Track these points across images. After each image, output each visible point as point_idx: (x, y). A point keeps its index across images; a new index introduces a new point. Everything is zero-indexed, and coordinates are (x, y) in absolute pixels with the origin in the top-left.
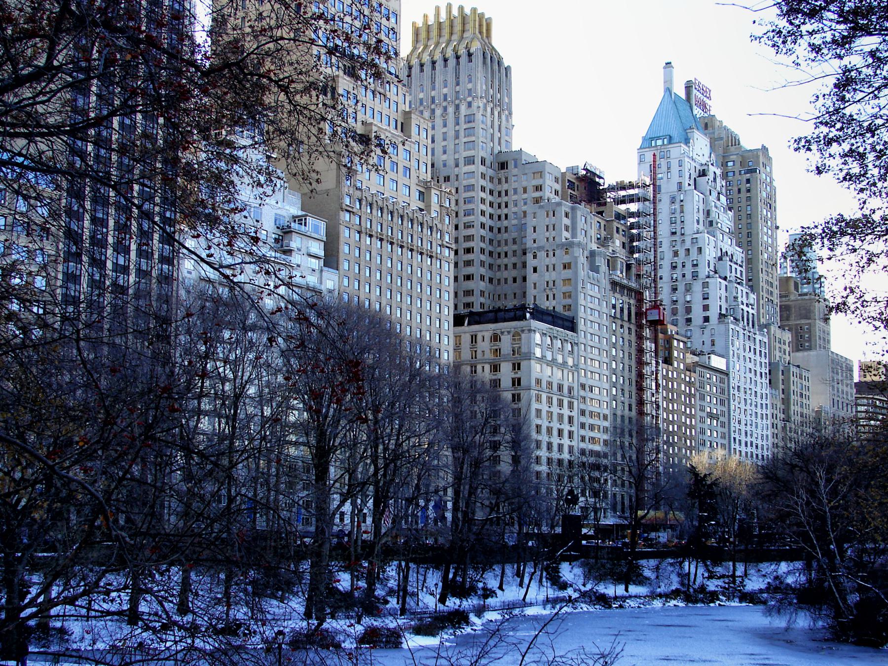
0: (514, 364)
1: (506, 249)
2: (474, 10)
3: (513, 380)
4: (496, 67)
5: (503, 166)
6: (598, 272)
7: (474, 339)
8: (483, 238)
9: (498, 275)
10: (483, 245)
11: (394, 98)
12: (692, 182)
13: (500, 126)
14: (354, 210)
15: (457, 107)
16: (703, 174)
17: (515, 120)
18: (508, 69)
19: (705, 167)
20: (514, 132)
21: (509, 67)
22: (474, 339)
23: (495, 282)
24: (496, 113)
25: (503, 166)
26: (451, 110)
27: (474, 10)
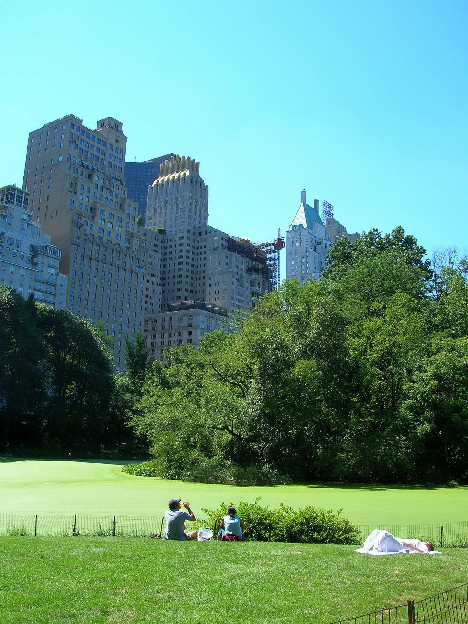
0: (189, 332)
1: (200, 276)
2: (189, 158)
3: (188, 340)
4: (199, 185)
5: (200, 234)
6: (243, 287)
7: (171, 319)
8: (187, 270)
9: (196, 289)
10: (187, 273)
11: (115, 191)
12: (313, 247)
13: (200, 214)
14: (81, 245)
15: (177, 205)
16: (319, 243)
17: (210, 211)
18: (207, 186)
19: (321, 241)
20: (209, 218)
21: (207, 186)
22: (171, 319)
23: (194, 292)
24: (198, 208)
25: (200, 234)
26: (175, 206)
27: (189, 158)
